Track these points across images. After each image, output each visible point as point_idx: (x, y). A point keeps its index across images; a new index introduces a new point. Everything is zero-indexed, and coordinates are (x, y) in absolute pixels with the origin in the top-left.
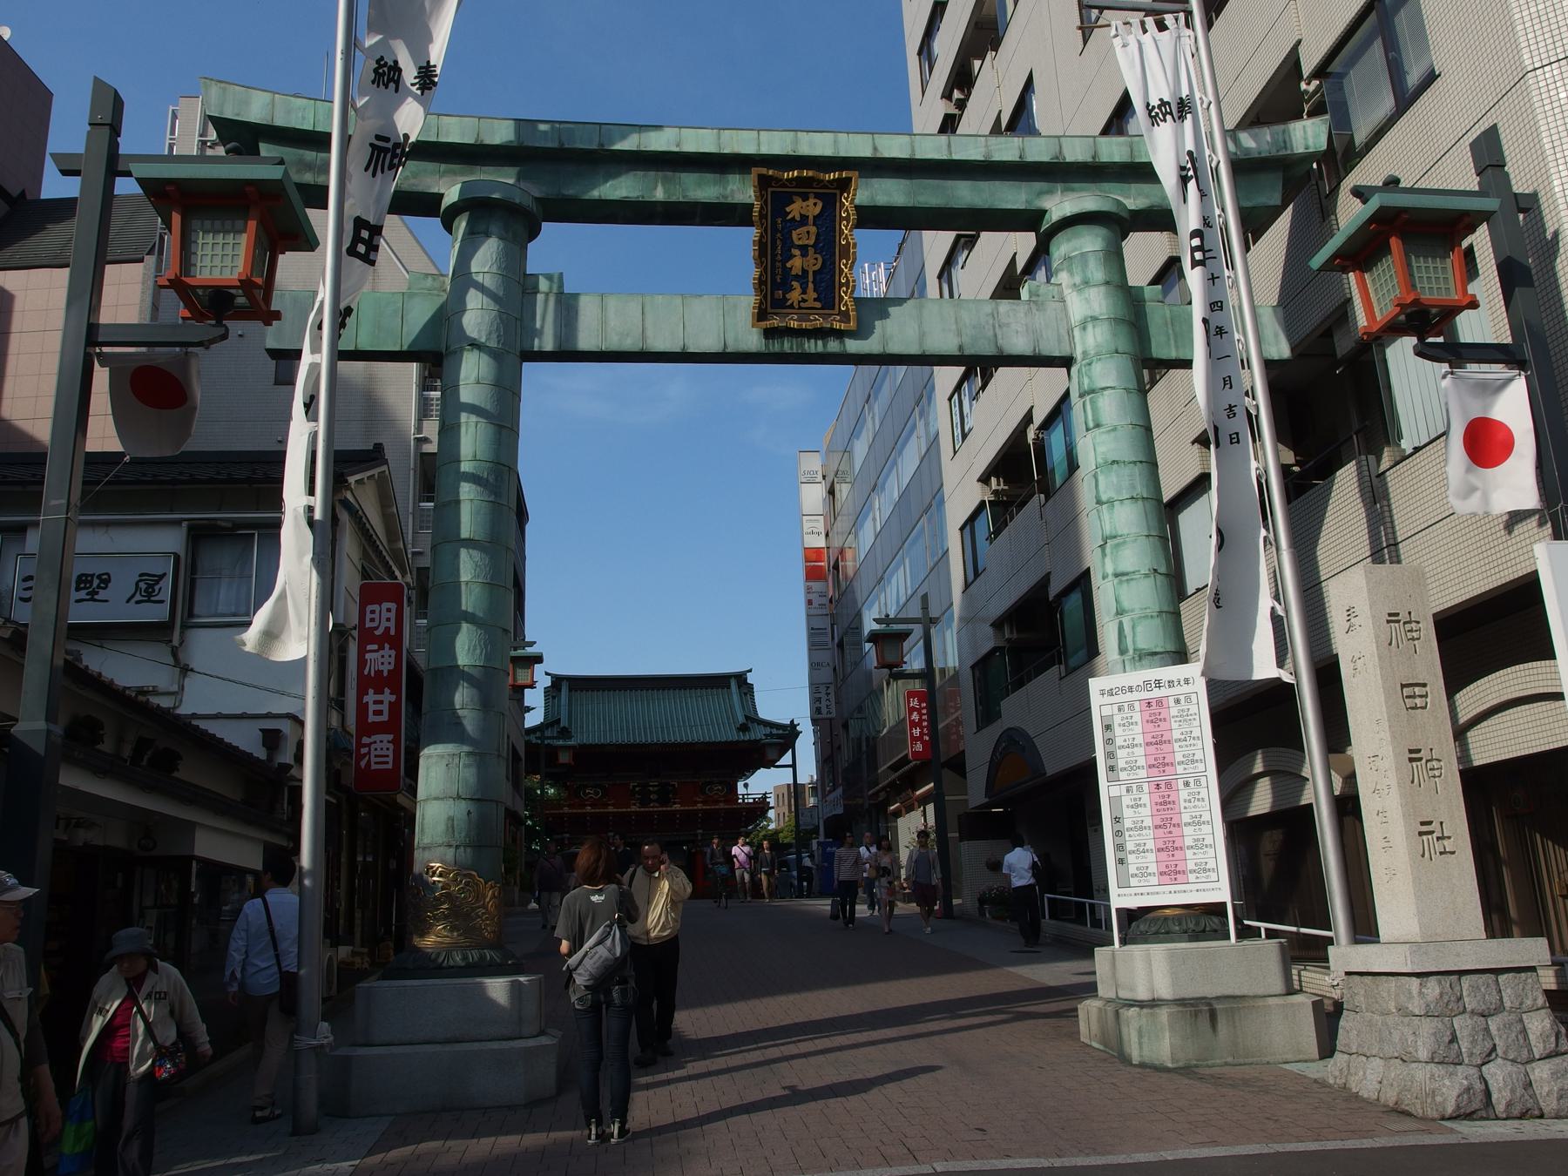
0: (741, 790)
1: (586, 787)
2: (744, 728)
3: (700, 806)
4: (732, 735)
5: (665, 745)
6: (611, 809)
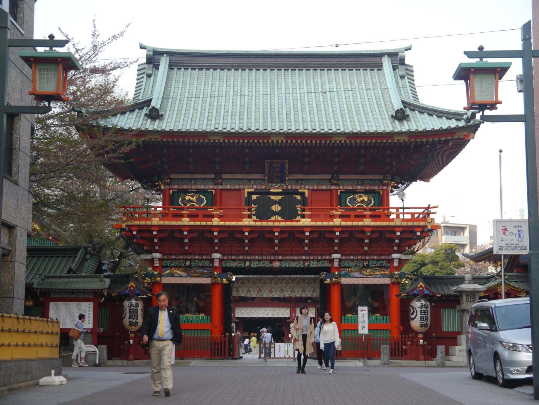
0: (394, 201)
1: (187, 192)
2: (400, 116)
3: (337, 222)
4: (383, 124)
5: (289, 136)
6: (216, 222)
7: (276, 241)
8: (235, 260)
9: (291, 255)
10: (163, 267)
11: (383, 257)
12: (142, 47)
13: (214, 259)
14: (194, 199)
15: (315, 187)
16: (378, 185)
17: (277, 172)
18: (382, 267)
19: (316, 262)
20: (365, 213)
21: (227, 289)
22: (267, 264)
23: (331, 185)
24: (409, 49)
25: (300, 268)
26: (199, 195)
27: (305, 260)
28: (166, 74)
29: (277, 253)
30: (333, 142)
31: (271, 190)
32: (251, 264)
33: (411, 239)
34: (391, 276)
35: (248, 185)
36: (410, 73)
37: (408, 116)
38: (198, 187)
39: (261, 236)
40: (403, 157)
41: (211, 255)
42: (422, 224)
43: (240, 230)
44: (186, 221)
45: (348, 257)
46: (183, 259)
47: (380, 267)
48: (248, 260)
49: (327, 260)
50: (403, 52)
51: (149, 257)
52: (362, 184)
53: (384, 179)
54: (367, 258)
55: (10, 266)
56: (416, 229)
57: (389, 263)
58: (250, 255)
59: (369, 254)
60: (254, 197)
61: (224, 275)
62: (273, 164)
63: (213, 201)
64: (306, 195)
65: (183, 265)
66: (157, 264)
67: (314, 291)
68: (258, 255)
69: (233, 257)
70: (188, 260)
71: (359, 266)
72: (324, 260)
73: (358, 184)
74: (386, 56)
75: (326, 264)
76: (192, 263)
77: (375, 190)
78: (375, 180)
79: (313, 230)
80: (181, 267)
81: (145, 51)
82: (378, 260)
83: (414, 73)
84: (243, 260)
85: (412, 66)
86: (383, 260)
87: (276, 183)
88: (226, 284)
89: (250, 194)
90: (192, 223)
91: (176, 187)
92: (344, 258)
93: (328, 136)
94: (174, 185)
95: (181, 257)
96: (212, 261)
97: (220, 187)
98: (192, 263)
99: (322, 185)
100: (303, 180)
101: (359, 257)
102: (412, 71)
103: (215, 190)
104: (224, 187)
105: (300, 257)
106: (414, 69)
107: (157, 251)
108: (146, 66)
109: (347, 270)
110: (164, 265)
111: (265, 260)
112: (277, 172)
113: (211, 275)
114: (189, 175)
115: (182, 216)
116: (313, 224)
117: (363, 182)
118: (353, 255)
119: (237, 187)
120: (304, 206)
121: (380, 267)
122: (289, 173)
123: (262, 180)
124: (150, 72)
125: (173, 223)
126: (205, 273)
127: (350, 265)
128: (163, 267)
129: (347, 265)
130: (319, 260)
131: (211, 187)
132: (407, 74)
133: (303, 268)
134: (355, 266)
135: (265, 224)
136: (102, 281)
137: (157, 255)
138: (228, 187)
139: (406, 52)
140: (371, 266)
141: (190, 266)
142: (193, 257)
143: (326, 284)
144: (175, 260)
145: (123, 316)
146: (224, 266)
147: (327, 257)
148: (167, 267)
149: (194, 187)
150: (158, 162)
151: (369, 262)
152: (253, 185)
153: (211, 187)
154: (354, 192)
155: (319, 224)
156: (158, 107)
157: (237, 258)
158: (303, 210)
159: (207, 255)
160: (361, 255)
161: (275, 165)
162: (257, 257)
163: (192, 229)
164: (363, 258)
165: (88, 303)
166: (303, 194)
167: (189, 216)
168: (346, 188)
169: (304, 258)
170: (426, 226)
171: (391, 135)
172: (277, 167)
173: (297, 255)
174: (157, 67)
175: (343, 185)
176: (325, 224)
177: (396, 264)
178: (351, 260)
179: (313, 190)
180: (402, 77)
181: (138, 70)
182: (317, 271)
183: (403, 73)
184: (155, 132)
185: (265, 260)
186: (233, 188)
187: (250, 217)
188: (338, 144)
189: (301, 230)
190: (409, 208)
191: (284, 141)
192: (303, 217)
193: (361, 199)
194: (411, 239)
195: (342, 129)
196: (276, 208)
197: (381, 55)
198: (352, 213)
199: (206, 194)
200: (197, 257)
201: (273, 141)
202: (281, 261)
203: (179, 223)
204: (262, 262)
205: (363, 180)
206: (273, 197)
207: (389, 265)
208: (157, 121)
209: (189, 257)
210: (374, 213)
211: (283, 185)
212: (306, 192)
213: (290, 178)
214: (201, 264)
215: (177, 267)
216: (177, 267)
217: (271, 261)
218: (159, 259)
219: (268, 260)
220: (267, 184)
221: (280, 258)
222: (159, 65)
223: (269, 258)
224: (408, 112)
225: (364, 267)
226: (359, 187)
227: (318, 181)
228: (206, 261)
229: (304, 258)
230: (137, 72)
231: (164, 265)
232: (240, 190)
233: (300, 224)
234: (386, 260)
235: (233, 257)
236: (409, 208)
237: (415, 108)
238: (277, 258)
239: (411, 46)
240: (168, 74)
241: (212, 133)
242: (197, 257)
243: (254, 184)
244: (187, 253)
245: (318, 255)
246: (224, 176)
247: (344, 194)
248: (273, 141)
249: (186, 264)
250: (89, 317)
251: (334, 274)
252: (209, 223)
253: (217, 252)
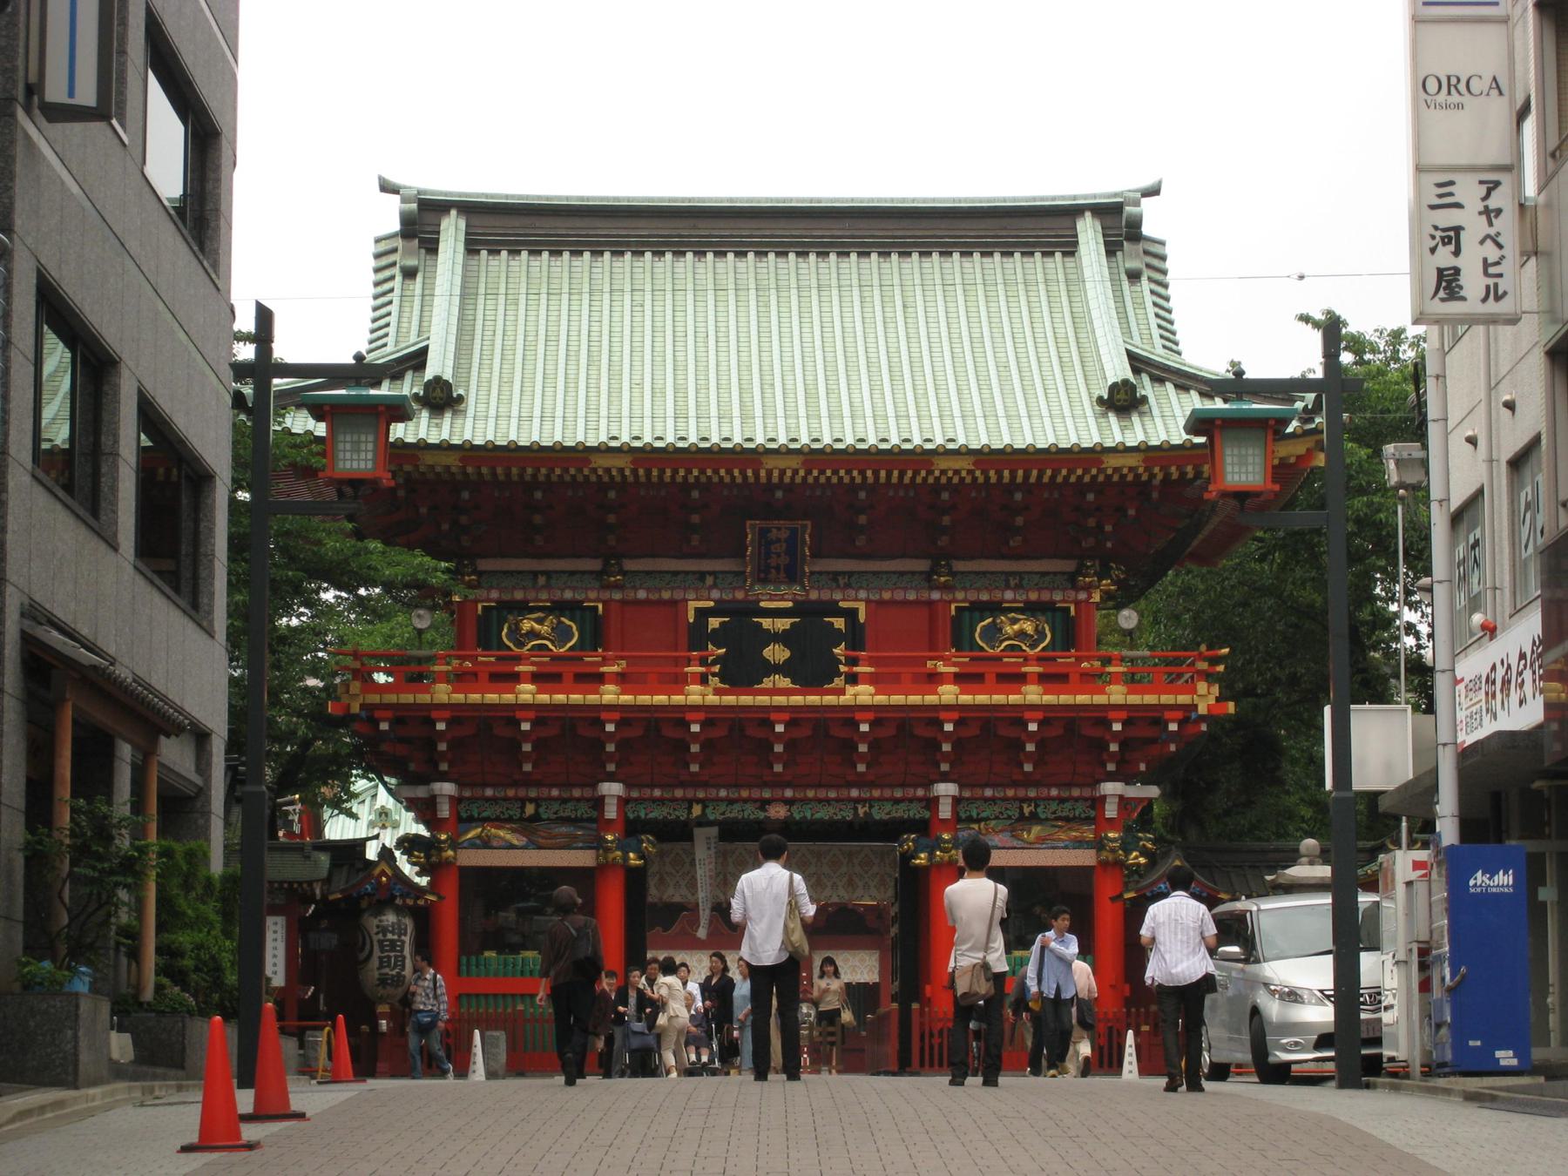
1: (523, 608)
2: (1122, 401)
3: (948, 693)
4: (1074, 424)
5: (816, 458)
6: (610, 694)
7: (779, 748)
8: (661, 801)
9: (819, 786)
10: (460, 820)
11: (1076, 792)
12: (387, 187)
13: (603, 797)
14: (544, 629)
15: (887, 596)
16: (1064, 590)
17: (779, 555)
18: (1074, 818)
19: (888, 806)
20: (1025, 669)
21: (635, 880)
22: (751, 812)
23: (931, 588)
24: (1153, 191)
25: (843, 822)
26: (558, 618)
27: (857, 801)
28: (459, 269)
29: (779, 783)
30: (937, 473)
31: (762, 604)
32: (708, 811)
33: (1153, 741)
34: (1099, 844)
35: (696, 590)
36: (1155, 262)
37: (1144, 399)
38: (557, 595)
39: (737, 735)
40: (1132, 512)
41: (594, 786)
42: (1183, 699)
43: (679, 717)
44: (527, 692)
45: (978, 792)
46: (516, 799)
47: (1067, 819)
48: (699, 801)
49: (920, 800)
50: (1137, 204)
51: (421, 792)
52: (1018, 587)
53: (1079, 571)
54: (1032, 793)
55: (201, 822)
56: (1167, 715)
57: (1093, 807)
58: (705, 785)
59: (1037, 784)
60: (714, 623)
61: (632, 841)
62: (769, 530)
63: (596, 634)
64: (862, 617)
65: (516, 814)
66: (444, 811)
68: (727, 786)
69: (657, 793)
71: (1009, 817)
72: (911, 800)
73: (1008, 587)
74: (1088, 214)
75: (916, 812)
76: (541, 810)
77: (1055, 603)
78: (1055, 574)
79: (879, 715)
80: (510, 820)
81: (397, 198)
82: (1061, 800)
83: (1168, 264)
84: (683, 800)
85: (1162, 243)
86: (1076, 800)
87: (777, 582)
88: (637, 868)
89: (703, 614)
90: (544, 698)
91: (494, 594)
92: (967, 794)
93: (921, 458)
94: (490, 588)
95: (511, 793)
96: (599, 803)
97: (617, 596)
98: (541, 810)
99: (905, 589)
100: (851, 574)
101: (1010, 793)
102: (1163, 258)
103: (605, 603)
104: (631, 595)
105: (844, 793)
106: (1168, 250)
107: (444, 777)
108: (399, 243)
109: (976, 826)
110: (464, 815)
111: (745, 801)
112: (779, 555)
113: (597, 844)
114: (527, 561)
115: (516, 678)
116: (881, 699)
117: (1022, 579)
118: (993, 786)
119: (666, 595)
120: (854, 649)
121: (1067, 819)
122: (813, 556)
123: (737, 574)
124: (411, 262)
125: (492, 698)
126: (576, 837)
127: (984, 815)
128: (464, 821)
129: (974, 814)
130: (897, 801)
131: (592, 595)
132: (1148, 266)
133: (850, 824)
134: (997, 818)
135: (746, 700)
136: (308, 858)
137: (448, 788)
138: (642, 595)
139: (1144, 201)
141: (536, 818)
142: (545, 792)
143: (917, 867)
144: (493, 800)
145: (362, 956)
146: (631, 816)
147: (920, 792)
148: (471, 821)
149: (544, 596)
150: (445, 527)
151: (1036, 806)
152: (710, 588)
153: (595, 599)
154: (995, 608)
155: (897, 699)
156: (448, 376)
157: (667, 795)
158: (853, 662)
159: (582, 786)
160: (1015, 784)
161: (774, 534)
162: (723, 793)
163: (542, 714)
164: (1021, 793)
166: (851, 614)
167: (535, 678)
168: (972, 596)
169: (854, 793)
171: (1095, 454)
172: (779, 540)
173: (837, 787)
174: (432, 247)
175: (964, 589)
176: (914, 699)
177: (1111, 811)
178: (986, 800)
179: (881, 603)
180: (1134, 276)
181: (377, 256)
182: (891, 830)
183: (1133, 264)
184: (445, 447)
185: (745, 801)
186: (654, 597)
187: (703, 680)
188: (950, 479)
189: (849, 716)
191: (802, 473)
192: (853, 679)
193: (1016, 627)
194: (1153, 741)
195: (961, 441)
196: (777, 653)
197: (1069, 213)
198: (990, 670)
199: (578, 613)
200: (555, 792)
201: (769, 473)
202: (789, 802)
203: (508, 698)
204: (737, 807)
205: (1020, 574)
206: (766, 623)
207: (1093, 814)
208: (448, 415)
209: (533, 794)
210: (1053, 670)
211: (797, 589)
212: (862, 608)
213: (817, 568)
214: (568, 812)
215: (499, 821)
216: (498, 819)
217: (764, 804)
218: (451, 797)
219: (755, 801)
220: (752, 586)
221: (789, 793)
222: (437, 241)
223: (756, 794)
224: (1146, 388)
225: (1022, 818)
226: (1009, 595)
227: (894, 578)
228: (582, 804)
229: (854, 793)
230: (372, 263)
231: (464, 815)
232: (673, 603)
233: (845, 699)
234: (1086, 799)
235: (657, 793)
237: (1162, 374)
238: (778, 793)
239: (1160, 183)
240: (465, 266)
241: (603, 450)
243: (715, 586)
244: (528, 781)
245: (892, 786)
246: (630, 565)
247: (967, 614)
248: (769, 473)
249: (523, 812)
251: (939, 839)
252: (592, 699)
253: (611, 778)
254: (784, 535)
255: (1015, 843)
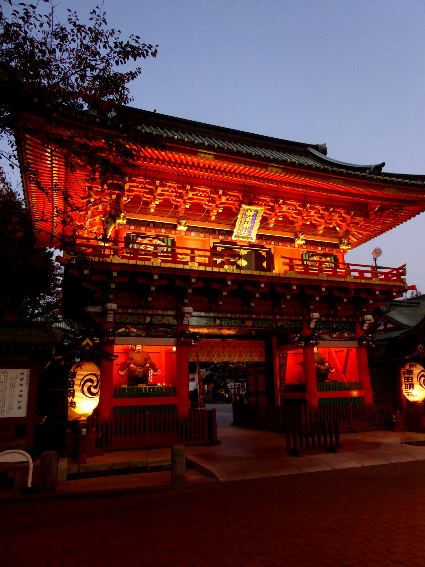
27: (278, 320)
32: (222, 322)
48: (218, 318)
67: (260, 356)
70: (149, 315)
71: (329, 328)
76: (153, 320)
127: (321, 327)
134: (325, 329)
140: (340, 328)
144: (132, 314)
151: (337, 325)
165: (18, 372)
170: (401, 287)
190: (382, 268)
200: (160, 312)
202: (253, 320)
215: (134, 325)
236: (382, 268)
242: (160, 312)
249: (145, 320)
250: (20, 396)
254: (252, 213)
255: (331, 338)
